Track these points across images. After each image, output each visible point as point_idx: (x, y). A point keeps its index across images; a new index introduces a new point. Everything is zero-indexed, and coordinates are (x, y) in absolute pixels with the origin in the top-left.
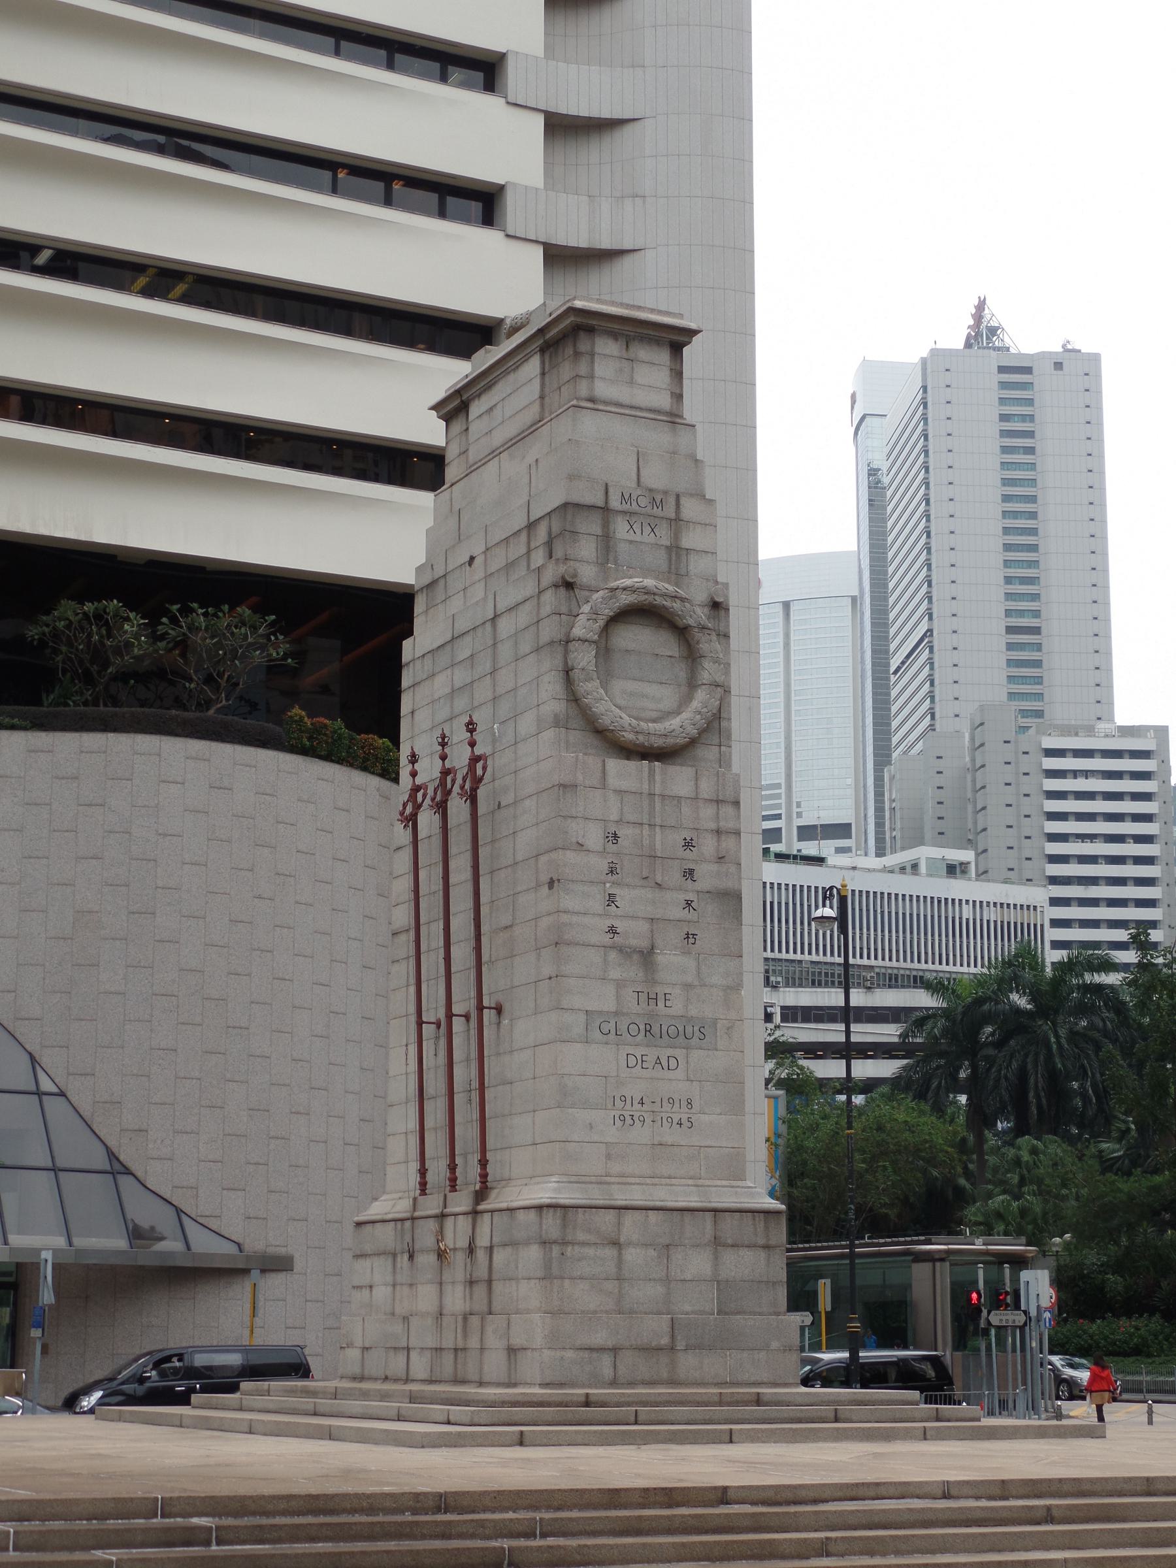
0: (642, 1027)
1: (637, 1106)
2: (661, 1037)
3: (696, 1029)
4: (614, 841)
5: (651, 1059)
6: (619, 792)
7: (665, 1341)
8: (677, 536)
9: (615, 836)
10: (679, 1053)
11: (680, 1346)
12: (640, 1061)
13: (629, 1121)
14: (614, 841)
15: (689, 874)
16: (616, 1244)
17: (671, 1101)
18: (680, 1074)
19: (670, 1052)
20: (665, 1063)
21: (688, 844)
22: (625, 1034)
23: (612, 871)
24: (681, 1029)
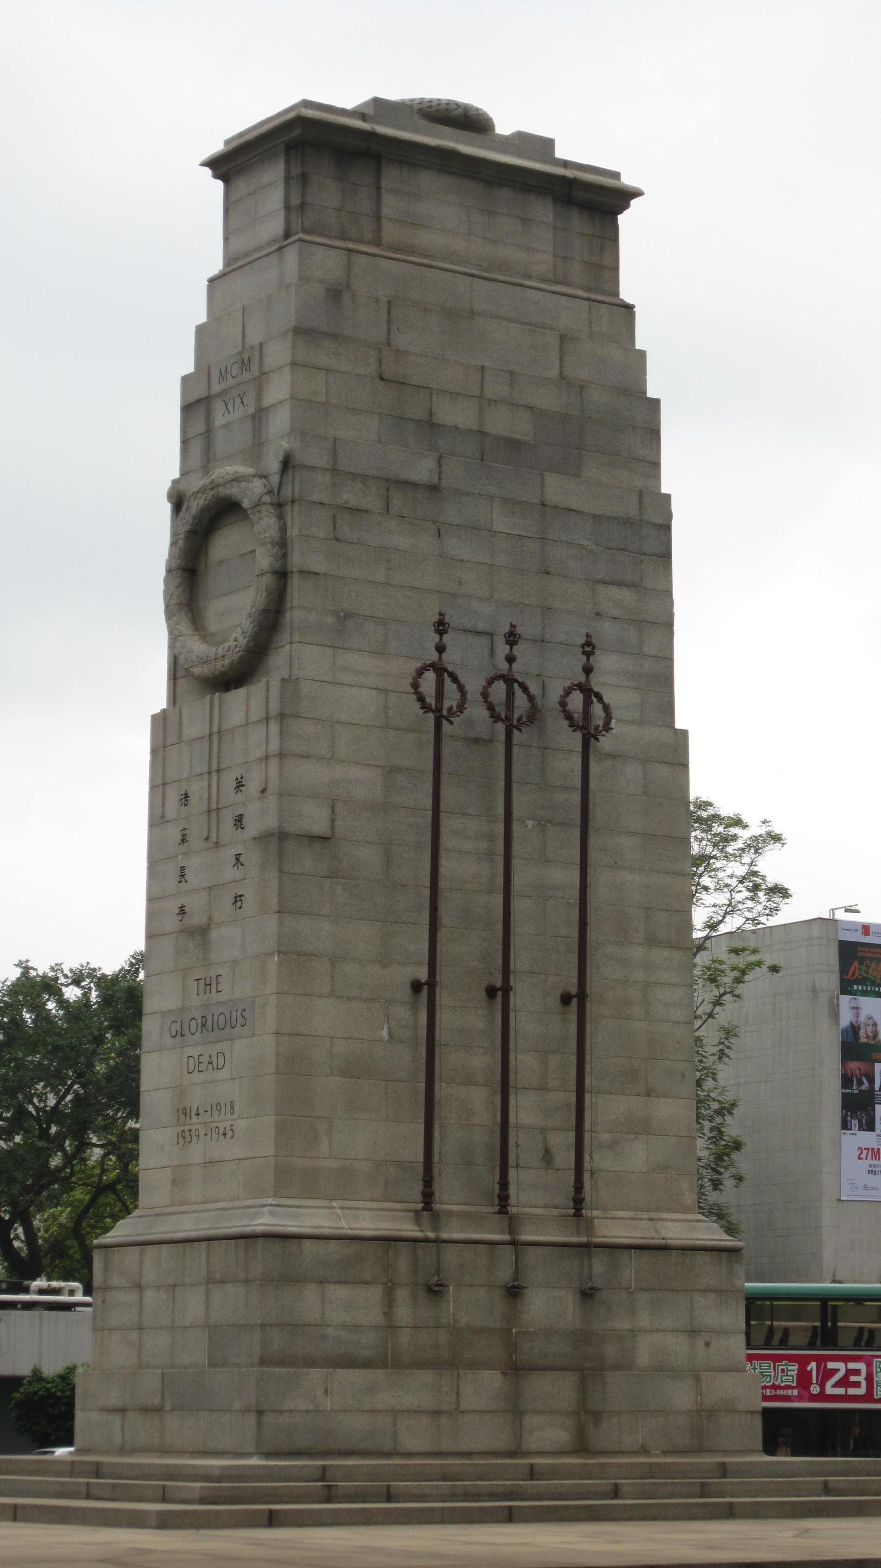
0: (199, 1021)
1: (194, 1118)
2: (213, 1031)
3: (239, 1013)
4: (186, 803)
5: (205, 1059)
6: (191, 741)
7: (156, 1401)
8: (259, 398)
9: (187, 796)
10: (224, 1046)
11: (168, 1407)
12: (197, 1064)
13: (188, 1138)
14: (186, 803)
15: (239, 821)
16: (139, 1287)
17: (219, 1108)
18: (223, 1074)
19: (219, 1047)
20: (215, 1062)
21: (239, 785)
22: (188, 1034)
23: (184, 840)
24: (228, 1016)
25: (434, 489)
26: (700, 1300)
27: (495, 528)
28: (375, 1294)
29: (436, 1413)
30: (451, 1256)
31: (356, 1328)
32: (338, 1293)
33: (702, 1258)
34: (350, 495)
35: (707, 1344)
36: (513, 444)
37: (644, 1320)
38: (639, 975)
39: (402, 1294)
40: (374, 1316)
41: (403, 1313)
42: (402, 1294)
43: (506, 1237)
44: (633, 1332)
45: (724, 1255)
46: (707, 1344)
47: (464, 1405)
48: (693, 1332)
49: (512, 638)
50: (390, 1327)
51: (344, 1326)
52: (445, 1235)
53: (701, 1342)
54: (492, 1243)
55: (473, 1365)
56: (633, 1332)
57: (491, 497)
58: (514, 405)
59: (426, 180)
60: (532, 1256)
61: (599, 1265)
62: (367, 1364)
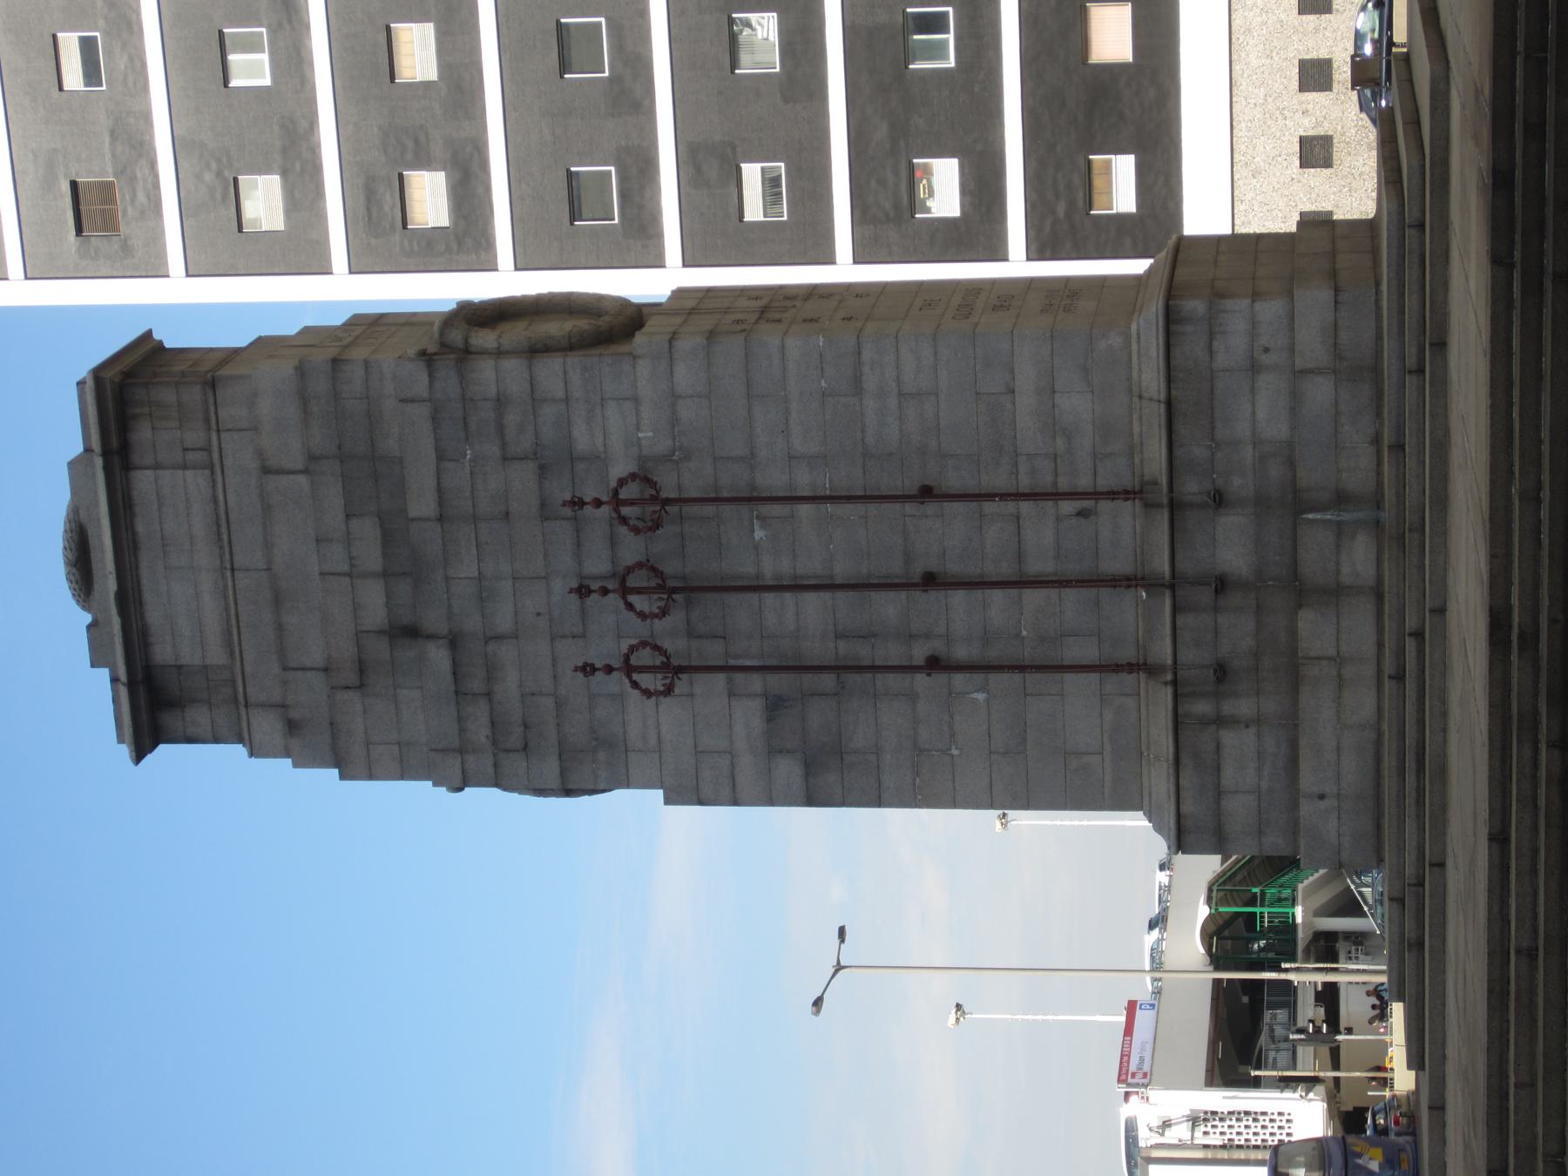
25: (454, 642)
26: (1221, 360)
27: (476, 574)
28: (1229, 738)
29: (1341, 682)
30: (1188, 655)
31: (1260, 755)
32: (1229, 775)
33: (1176, 353)
34: (480, 732)
35: (1266, 350)
36: (388, 539)
37: (1242, 429)
38: (893, 402)
39: (1228, 708)
40: (1249, 736)
41: (1243, 707)
42: (1228, 708)
43: (1168, 593)
44: (1256, 442)
45: (1173, 328)
46: (1266, 350)
47: (1332, 652)
48: (1254, 368)
49: (583, 591)
50: (1257, 721)
51: (1259, 769)
52: (1169, 662)
53: (1266, 359)
54: (1175, 610)
55: (1293, 633)
56: (1256, 442)
57: (447, 578)
58: (348, 540)
59: (154, 616)
60: (1186, 566)
61: (1191, 487)
62: (1294, 745)
